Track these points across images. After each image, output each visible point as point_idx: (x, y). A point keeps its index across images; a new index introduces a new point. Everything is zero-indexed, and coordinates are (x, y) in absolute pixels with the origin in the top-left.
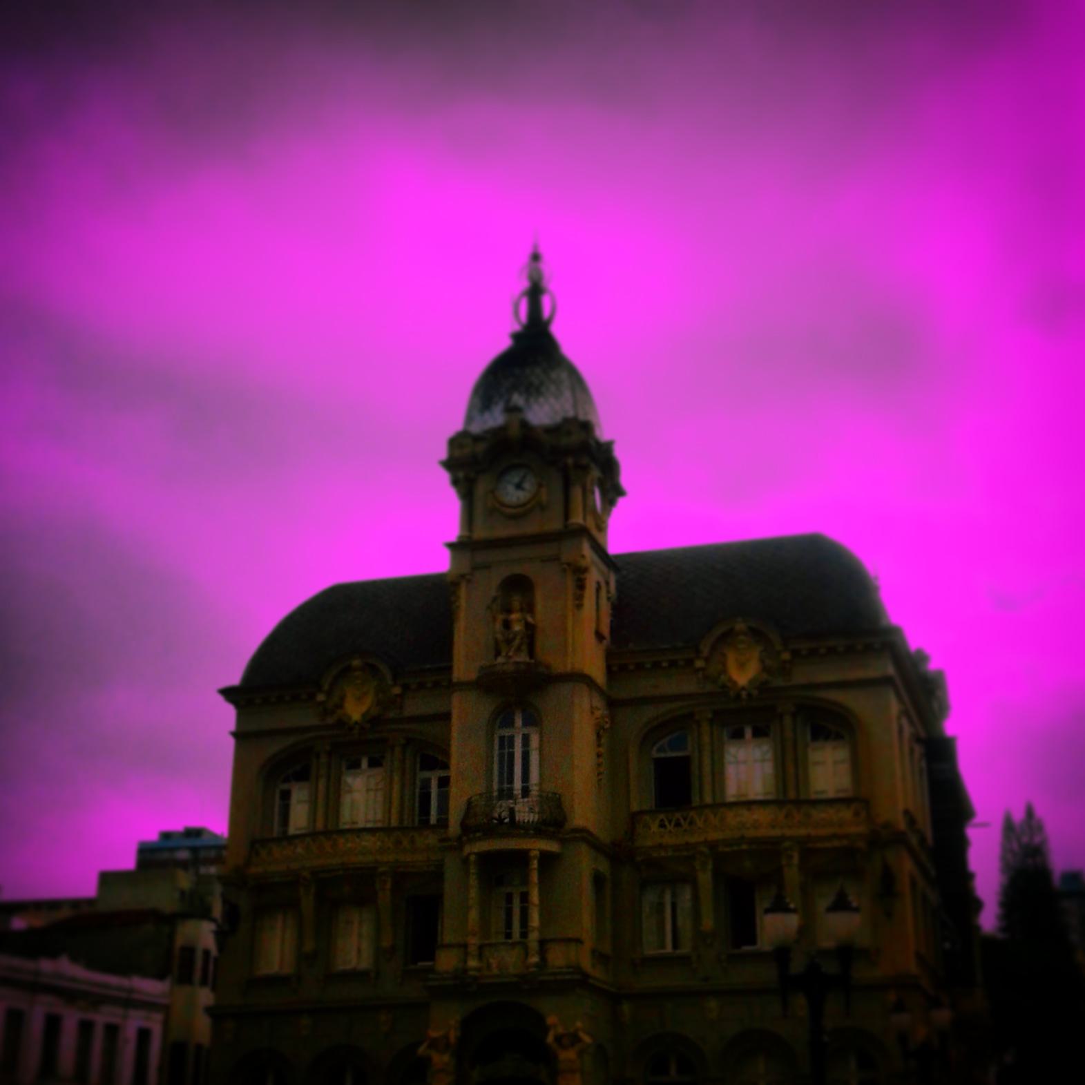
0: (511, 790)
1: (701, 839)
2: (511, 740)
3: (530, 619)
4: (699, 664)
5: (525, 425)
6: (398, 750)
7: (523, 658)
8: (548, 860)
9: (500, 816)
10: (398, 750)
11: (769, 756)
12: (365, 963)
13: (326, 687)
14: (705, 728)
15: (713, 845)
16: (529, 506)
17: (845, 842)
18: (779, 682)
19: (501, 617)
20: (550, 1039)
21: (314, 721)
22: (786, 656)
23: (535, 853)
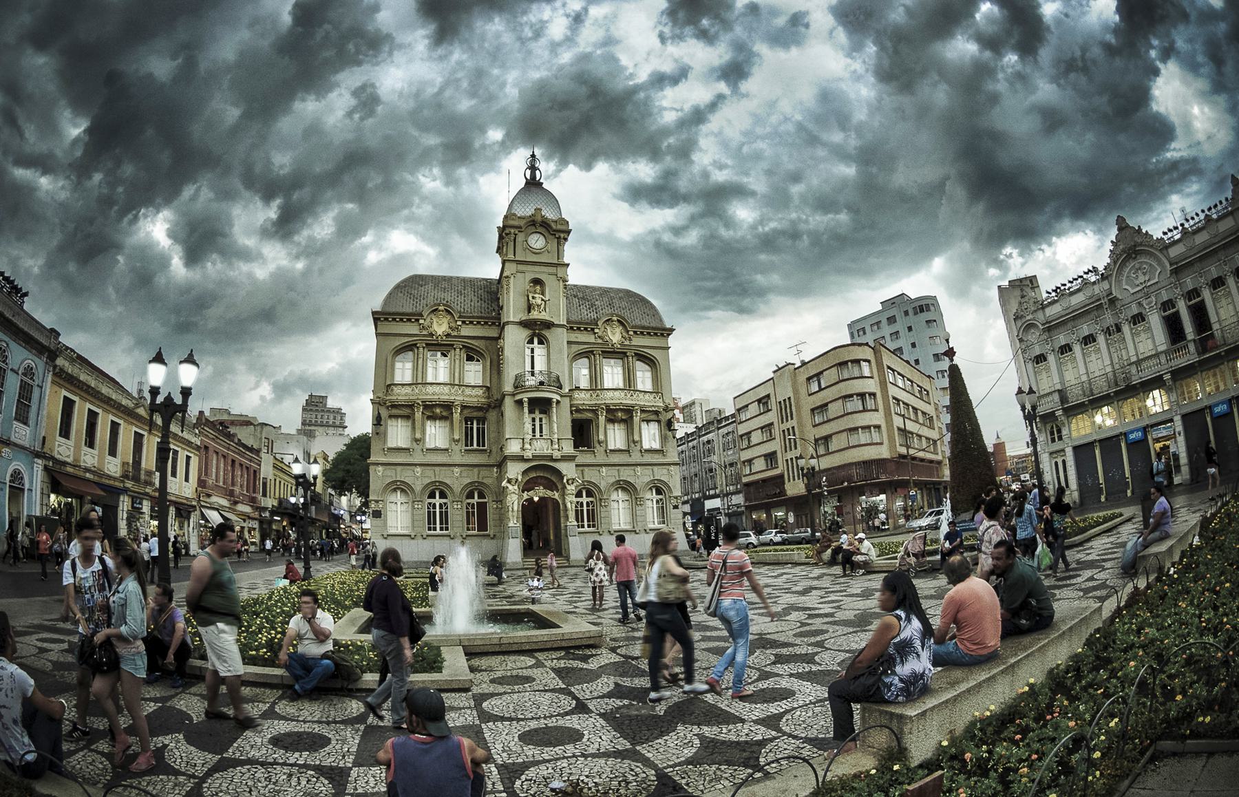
4: (596, 331)
8: (558, 402)
15: (607, 406)
18: (627, 343)
20: (565, 481)
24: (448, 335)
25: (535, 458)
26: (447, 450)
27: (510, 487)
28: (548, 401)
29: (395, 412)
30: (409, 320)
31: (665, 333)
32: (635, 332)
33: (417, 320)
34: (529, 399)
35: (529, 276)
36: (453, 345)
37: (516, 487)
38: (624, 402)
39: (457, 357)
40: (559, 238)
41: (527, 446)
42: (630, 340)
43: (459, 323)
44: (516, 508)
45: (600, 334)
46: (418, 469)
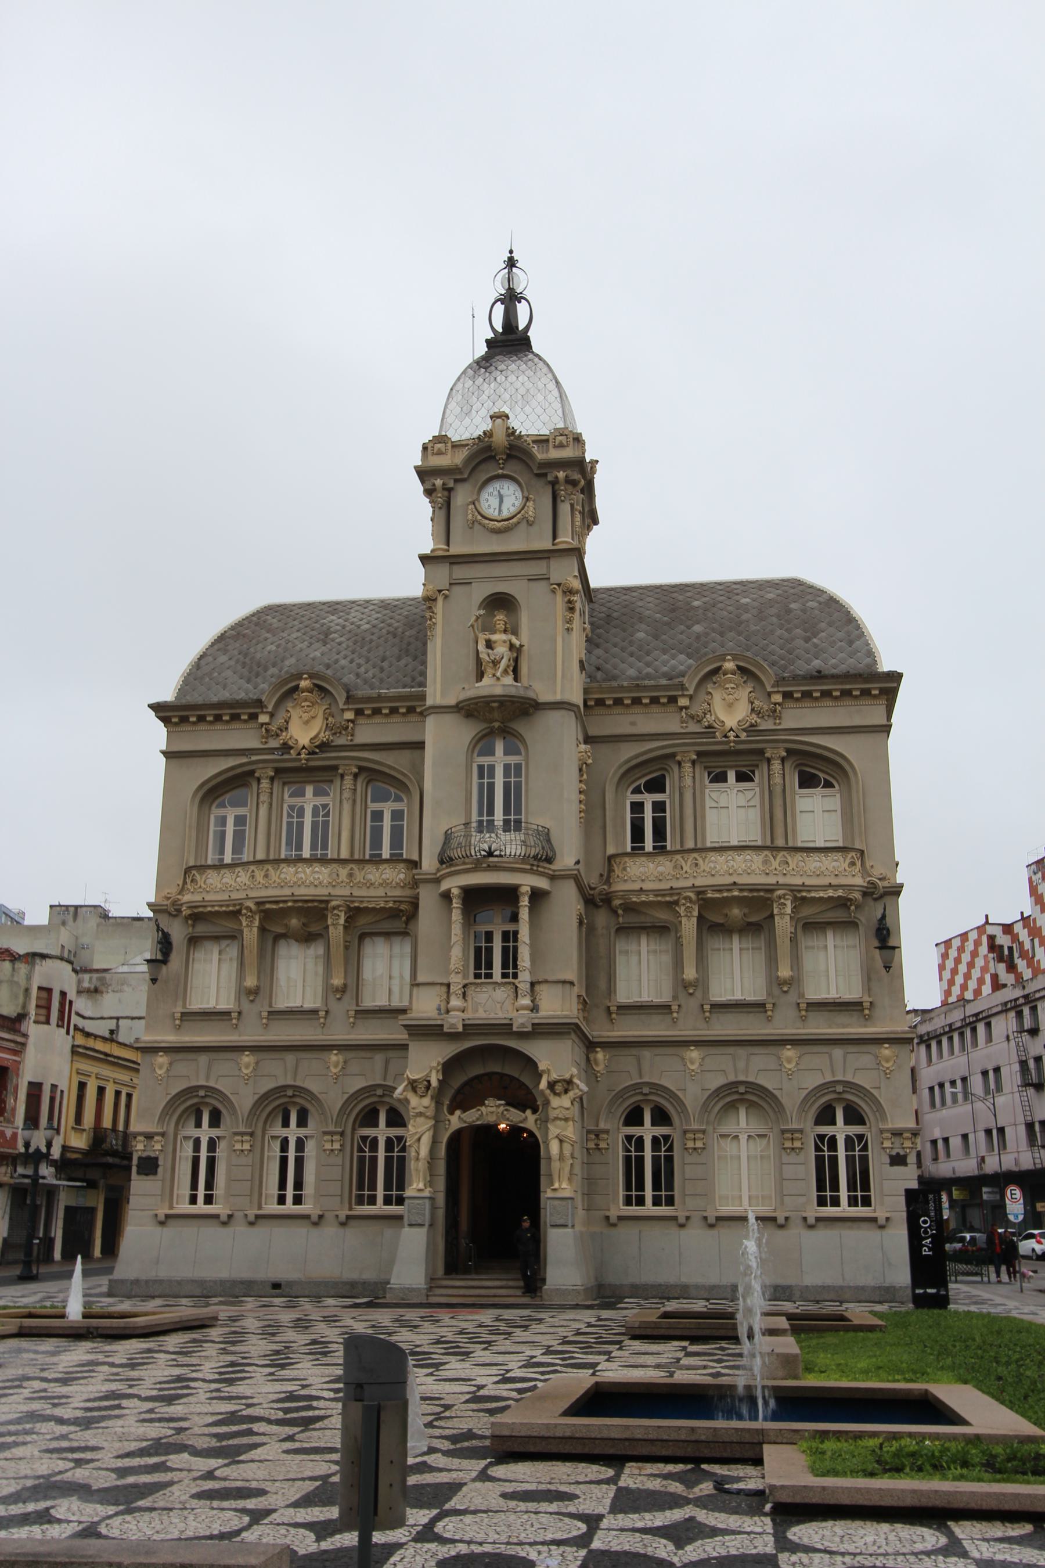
0: (491, 823)
1: (688, 883)
2: (492, 768)
3: (517, 643)
4: (683, 702)
5: (511, 433)
6: (348, 779)
7: (509, 680)
8: (537, 896)
9: (490, 848)
10: (348, 779)
11: (756, 801)
12: (311, 1001)
13: (270, 709)
14: (687, 767)
15: (700, 892)
16: (515, 520)
17: (840, 893)
18: (767, 725)
19: (482, 638)
20: (543, 1084)
21: (255, 743)
22: (778, 698)
23: (525, 889)
24: (324, 746)
25: (470, 1029)
26: (314, 1012)
27: (414, 1101)
28: (508, 895)
29: (201, 929)
30: (235, 717)
31: (875, 688)
32: (787, 695)
33: (254, 717)
34: (462, 888)
35: (481, 591)
36: (335, 768)
37: (426, 1101)
38: (741, 880)
39: (347, 794)
40: (554, 483)
41: (455, 1002)
42: (774, 714)
43: (349, 715)
44: (424, 1150)
45: (692, 711)
46: (247, 1058)
